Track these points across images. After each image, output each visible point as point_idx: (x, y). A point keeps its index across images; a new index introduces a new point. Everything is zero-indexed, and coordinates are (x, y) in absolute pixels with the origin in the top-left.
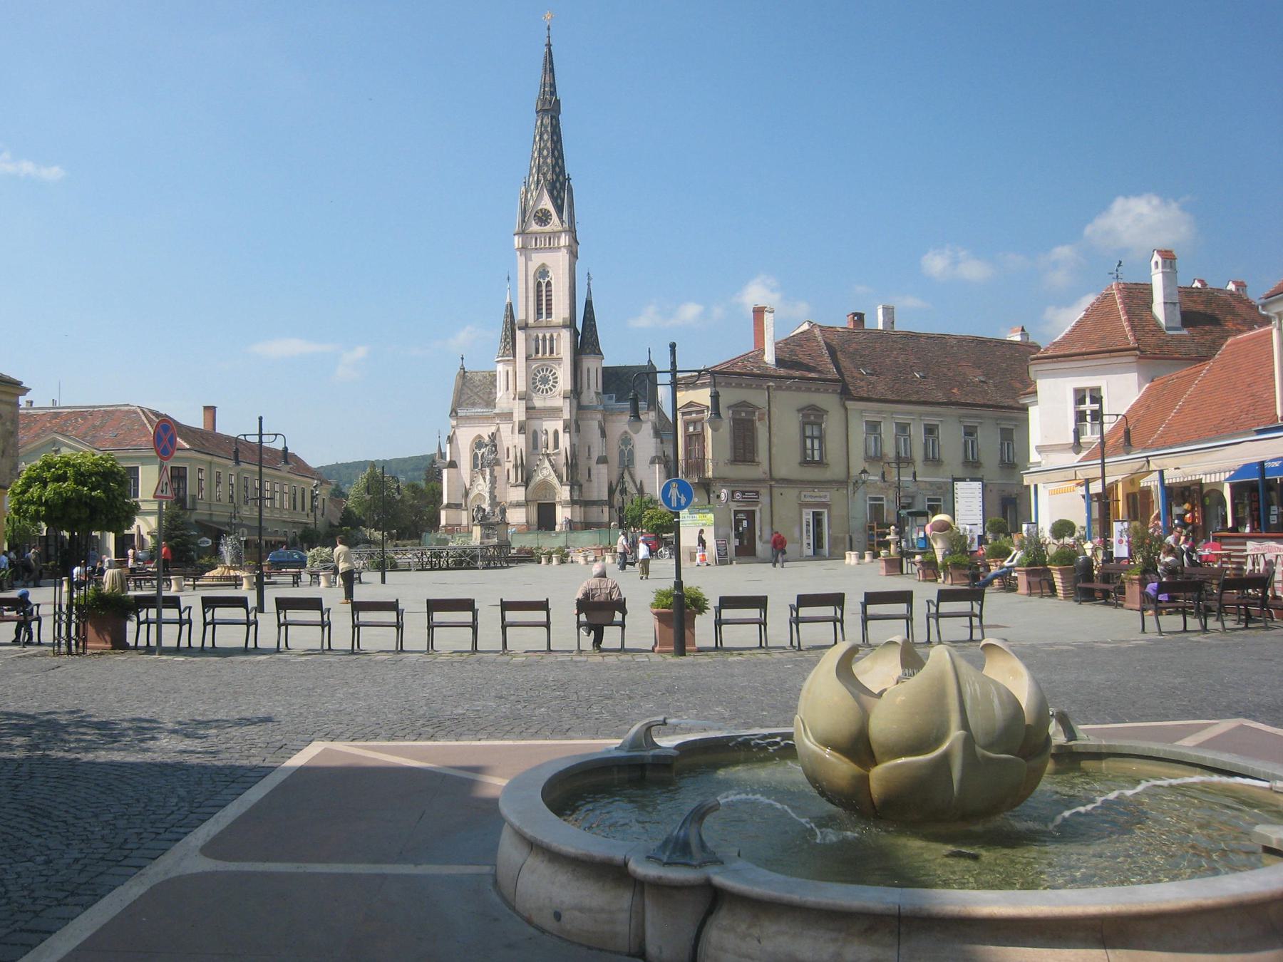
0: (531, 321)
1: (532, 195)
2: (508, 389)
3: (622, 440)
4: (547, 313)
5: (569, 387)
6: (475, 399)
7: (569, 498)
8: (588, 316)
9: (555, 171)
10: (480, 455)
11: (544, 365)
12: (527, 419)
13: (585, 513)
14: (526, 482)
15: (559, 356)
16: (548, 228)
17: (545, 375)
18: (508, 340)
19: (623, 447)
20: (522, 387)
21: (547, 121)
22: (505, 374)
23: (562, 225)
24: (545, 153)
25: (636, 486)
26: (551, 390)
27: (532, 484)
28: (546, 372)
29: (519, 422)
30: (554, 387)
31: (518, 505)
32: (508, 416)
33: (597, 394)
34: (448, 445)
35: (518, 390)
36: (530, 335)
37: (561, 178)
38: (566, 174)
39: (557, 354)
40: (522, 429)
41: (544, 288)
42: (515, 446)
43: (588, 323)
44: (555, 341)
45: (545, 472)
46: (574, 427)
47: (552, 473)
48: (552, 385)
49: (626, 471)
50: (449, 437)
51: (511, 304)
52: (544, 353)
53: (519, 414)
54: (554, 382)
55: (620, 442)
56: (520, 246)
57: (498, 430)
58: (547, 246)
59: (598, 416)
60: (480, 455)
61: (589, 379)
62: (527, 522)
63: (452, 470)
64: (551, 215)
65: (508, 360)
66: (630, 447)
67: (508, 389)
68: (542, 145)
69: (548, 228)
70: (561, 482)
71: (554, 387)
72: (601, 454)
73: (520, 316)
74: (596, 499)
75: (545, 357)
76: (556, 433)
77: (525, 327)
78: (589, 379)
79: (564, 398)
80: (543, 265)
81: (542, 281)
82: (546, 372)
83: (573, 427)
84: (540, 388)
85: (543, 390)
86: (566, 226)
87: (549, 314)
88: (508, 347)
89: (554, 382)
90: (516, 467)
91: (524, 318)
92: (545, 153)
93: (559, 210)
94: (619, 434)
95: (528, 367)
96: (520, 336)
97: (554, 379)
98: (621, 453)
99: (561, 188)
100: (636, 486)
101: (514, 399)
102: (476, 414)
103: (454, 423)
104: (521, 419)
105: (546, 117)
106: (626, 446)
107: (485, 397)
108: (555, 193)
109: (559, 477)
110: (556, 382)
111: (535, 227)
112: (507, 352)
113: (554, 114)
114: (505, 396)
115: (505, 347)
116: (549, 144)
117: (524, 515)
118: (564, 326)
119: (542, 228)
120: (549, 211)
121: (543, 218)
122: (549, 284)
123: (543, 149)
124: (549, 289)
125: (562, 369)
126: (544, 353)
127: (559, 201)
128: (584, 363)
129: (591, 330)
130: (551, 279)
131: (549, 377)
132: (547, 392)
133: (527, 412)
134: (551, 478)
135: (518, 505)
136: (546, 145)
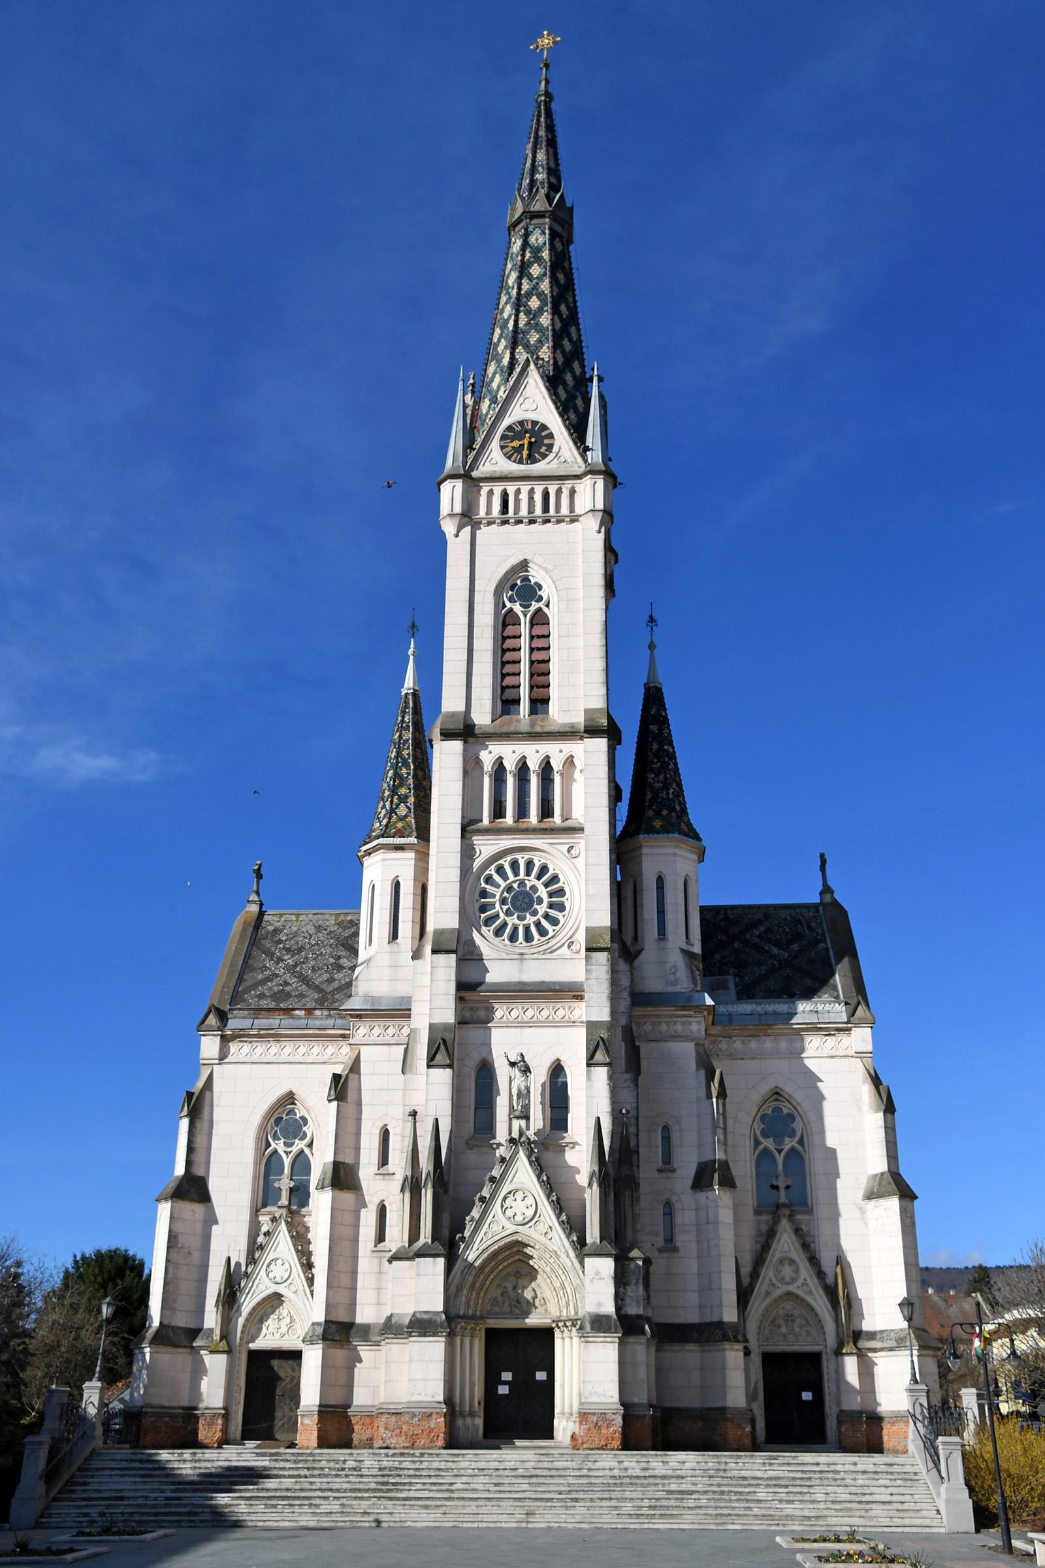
0: (482, 716)
2: (394, 936)
3: (763, 1118)
5: (603, 918)
6: (286, 983)
7: (609, 1308)
8: (653, 728)
9: (562, 347)
10: (287, 1162)
12: (462, 1022)
13: (661, 1372)
15: (568, 823)
17: (522, 883)
18: (403, 791)
19: (769, 1143)
24: (534, 303)
25: (820, 1274)
26: (542, 932)
27: (473, 1254)
28: (528, 874)
29: (431, 1026)
30: (554, 922)
32: (400, 1012)
33: (687, 953)
34: (184, 1124)
35: (430, 927)
37: (576, 365)
41: (524, 629)
42: (414, 1114)
43: (655, 746)
48: (547, 916)
49: (784, 1223)
52: (522, 811)
54: (551, 906)
55: (758, 1127)
56: (458, 509)
57: (355, 1067)
58: (538, 511)
59: (694, 1027)
60: (287, 1162)
61: (661, 912)
62: (449, 1401)
64: (551, 436)
66: (789, 1144)
67: (394, 936)
68: (526, 286)
69: (541, 467)
70: (580, 1244)
71: (554, 922)
72: (708, 1157)
73: (452, 701)
74: (692, 1317)
75: (523, 824)
76: (557, 1070)
77: (465, 732)
78: (661, 912)
79: (588, 949)
81: (517, 608)
82: (528, 874)
83: (621, 1049)
86: (595, 456)
87: (540, 703)
88: (402, 810)
89: (551, 906)
90: (413, 1186)
91: (462, 708)
92: (534, 303)
93: (578, 432)
94: (757, 1096)
97: (551, 895)
98: (764, 1158)
99: (576, 387)
100: (820, 1274)
101: (417, 955)
104: (437, 1020)
105: (538, 231)
106: (779, 1141)
107: (320, 978)
109: (574, 1227)
110: (561, 907)
111: (495, 460)
112: (400, 825)
113: (558, 229)
115: (392, 811)
116: (545, 286)
118: (592, 731)
119: (522, 467)
120: (544, 427)
122: (540, 619)
123: (529, 295)
124: (538, 630)
125: (580, 862)
126: (522, 811)
127: (572, 416)
129: (665, 766)
130: (548, 606)
132: (528, 938)
133: (460, 999)
134: (542, 1227)
136: (536, 287)
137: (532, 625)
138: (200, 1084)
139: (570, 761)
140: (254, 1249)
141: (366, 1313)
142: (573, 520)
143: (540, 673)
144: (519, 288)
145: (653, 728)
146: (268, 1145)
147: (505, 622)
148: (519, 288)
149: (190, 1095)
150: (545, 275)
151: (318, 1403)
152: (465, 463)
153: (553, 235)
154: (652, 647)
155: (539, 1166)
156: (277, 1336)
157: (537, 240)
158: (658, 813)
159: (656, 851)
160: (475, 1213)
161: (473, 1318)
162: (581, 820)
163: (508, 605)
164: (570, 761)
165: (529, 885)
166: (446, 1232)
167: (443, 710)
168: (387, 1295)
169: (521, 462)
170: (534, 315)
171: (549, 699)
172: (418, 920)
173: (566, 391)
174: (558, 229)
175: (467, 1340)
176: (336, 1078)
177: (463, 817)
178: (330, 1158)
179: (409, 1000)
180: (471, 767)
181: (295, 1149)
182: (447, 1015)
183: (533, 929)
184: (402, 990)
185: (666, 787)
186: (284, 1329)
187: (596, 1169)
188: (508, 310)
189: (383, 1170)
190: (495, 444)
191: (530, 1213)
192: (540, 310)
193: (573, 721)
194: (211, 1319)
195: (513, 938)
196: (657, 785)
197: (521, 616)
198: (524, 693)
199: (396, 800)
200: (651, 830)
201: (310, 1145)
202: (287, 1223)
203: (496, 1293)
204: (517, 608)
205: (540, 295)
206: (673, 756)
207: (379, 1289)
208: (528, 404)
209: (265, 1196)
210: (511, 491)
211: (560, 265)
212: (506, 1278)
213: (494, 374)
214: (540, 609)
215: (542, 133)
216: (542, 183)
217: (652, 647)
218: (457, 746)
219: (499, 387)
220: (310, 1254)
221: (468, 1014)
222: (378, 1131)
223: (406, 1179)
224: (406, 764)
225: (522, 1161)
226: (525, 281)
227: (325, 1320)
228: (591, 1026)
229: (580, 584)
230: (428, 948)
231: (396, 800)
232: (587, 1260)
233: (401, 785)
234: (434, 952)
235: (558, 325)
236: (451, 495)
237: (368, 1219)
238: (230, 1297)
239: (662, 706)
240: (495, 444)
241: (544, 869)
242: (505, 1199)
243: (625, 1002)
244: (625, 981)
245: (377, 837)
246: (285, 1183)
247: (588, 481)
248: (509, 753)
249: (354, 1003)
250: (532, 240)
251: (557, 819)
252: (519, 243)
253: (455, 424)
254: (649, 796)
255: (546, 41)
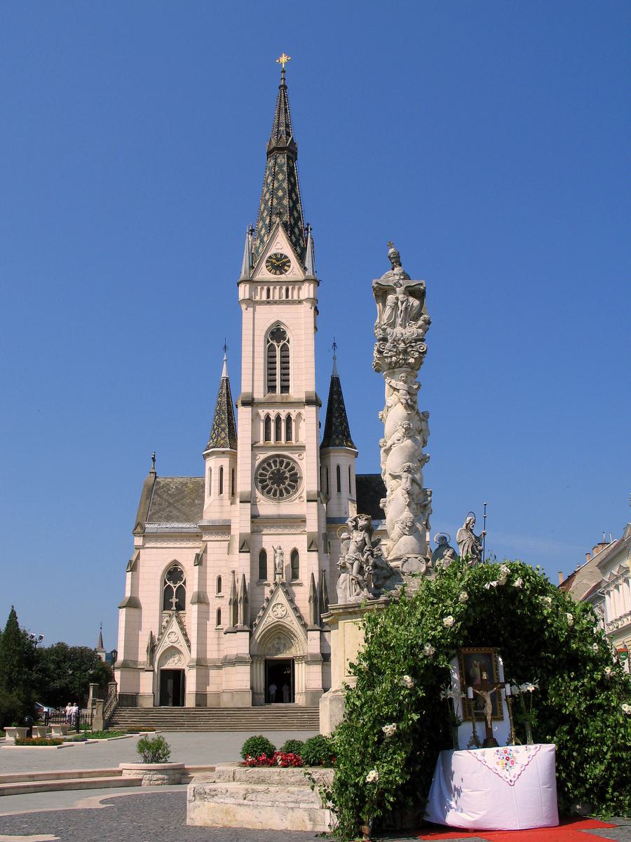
0: (259, 394)
1: (262, 241)
2: (221, 492)
4: (282, 387)
8: (335, 397)
9: (293, 215)
10: (175, 590)
11: (278, 456)
12: (253, 532)
14: (250, 626)
15: (298, 444)
16: (283, 277)
17: (279, 470)
18: (223, 426)
20: (244, 483)
21: (282, 160)
22: (218, 471)
23: (305, 273)
24: (280, 193)
29: (240, 534)
31: (237, 661)
34: (129, 575)
36: (258, 414)
38: (306, 223)
39: (297, 441)
40: (245, 546)
41: (278, 353)
42: (233, 572)
43: (336, 406)
44: (293, 424)
45: (278, 612)
46: (325, 542)
47: (291, 612)
48: (289, 485)
50: (131, 561)
51: (227, 380)
52: (278, 438)
53: (241, 523)
57: (205, 551)
60: (175, 590)
62: (252, 688)
63: (133, 611)
64: (289, 261)
65: (223, 452)
67: (221, 492)
68: (276, 185)
69: (283, 277)
70: (305, 625)
73: (246, 388)
77: (250, 402)
79: (308, 501)
80: (278, 323)
81: (275, 344)
84: (271, 489)
85: (276, 491)
86: (309, 273)
87: (285, 388)
88: (223, 435)
90: (234, 603)
92: (280, 193)
93: (301, 257)
95: (254, 457)
96: (243, 416)
102: (172, 530)
103: (138, 541)
108: (294, 240)
111: (264, 274)
112: (222, 442)
114: (217, 503)
116: (285, 185)
117: (248, 677)
118: (309, 402)
120: (286, 257)
121: (279, 264)
122: (285, 349)
123: (278, 189)
126: (278, 438)
128: (331, 460)
130: (288, 342)
131: (284, 473)
133: (252, 522)
135: (237, 661)
137: (281, 351)
138: (134, 558)
139: (299, 415)
140: (163, 629)
141: (212, 654)
142: (300, 302)
143: (285, 376)
144: (273, 186)
145: (335, 397)
146: (166, 583)
147: (271, 349)
148: (273, 186)
149: (131, 561)
150: (285, 179)
151: (195, 690)
152: (250, 274)
153: (289, 158)
154: (334, 358)
155: (287, 593)
156: (173, 664)
157: (281, 161)
158: (337, 437)
159: (336, 454)
160: (261, 613)
161: (261, 656)
162: (304, 442)
163: (271, 342)
164: (299, 415)
165: (281, 471)
166: (249, 621)
167: (243, 391)
168: (222, 647)
169: (275, 274)
170: (280, 199)
171: (289, 387)
172: (231, 485)
173: (296, 237)
174: (290, 154)
175: (258, 665)
176: (199, 554)
177: (252, 441)
178: (196, 589)
179: (230, 520)
180: (255, 417)
181: (178, 585)
182: (247, 529)
183: (284, 491)
184: (225, 516)
185: (341, 424)
186: (176, 661)
187: (312, 594)
188: (268, 196)
189: (220, 594)
190: (264, 264)
191: (284, 613)
192: (284, 196)
193: (300, 396)
194: (143, 657)
195: (275, 495)
196: (337, 424)
197: (277, 347)
198: (278, 384)
199: (220, 430)
200: (335, 445)
201: (184, 583)
202: (176, 617)
203: (270, 645)
204: (275, 344)
205: (283, 189)
206: (344, 410)
207: (219, 644)
208: (278, 246)
209: (166, 605)
210: (271, 288)
211: (291, 173)
212: (274, 640)
213: (262, 227)
214: (285, 344)
215: (282, 106)
216: (283, 132)
217: (334, 358)
218: (249, 409)
219: (264, 235)
220: (185, 630)
221: (256, 528)
222: (216, 578)
223: (231, 600)
224: (224, 413)
225: (281, 593)
226: (275, 182)
227: (197, 658)
228: (310, 535)
229: (303, 332)
230: (238, 500)
231: (220, 430)
232: (309, 632)
233: (222, 423)
234: (241, 502)
235: (291, 204)
236: (244, 291)
237: (213, 615)
238: (152, 649)
239: (339, 386)
240: (264, 264)
241: (288, 464)
242: (274, 607)
243: (324, 524)
244: (323, 515)
245: (214, 447)
246: (174, 600)
247: (306, 284)
248: (273, 413)
249: (204, 523)
250: (279, 161)
251: (293, 441)
252: (272, 161)
253: (244, 260)
254: (333, 428)
255: (284, 59)
